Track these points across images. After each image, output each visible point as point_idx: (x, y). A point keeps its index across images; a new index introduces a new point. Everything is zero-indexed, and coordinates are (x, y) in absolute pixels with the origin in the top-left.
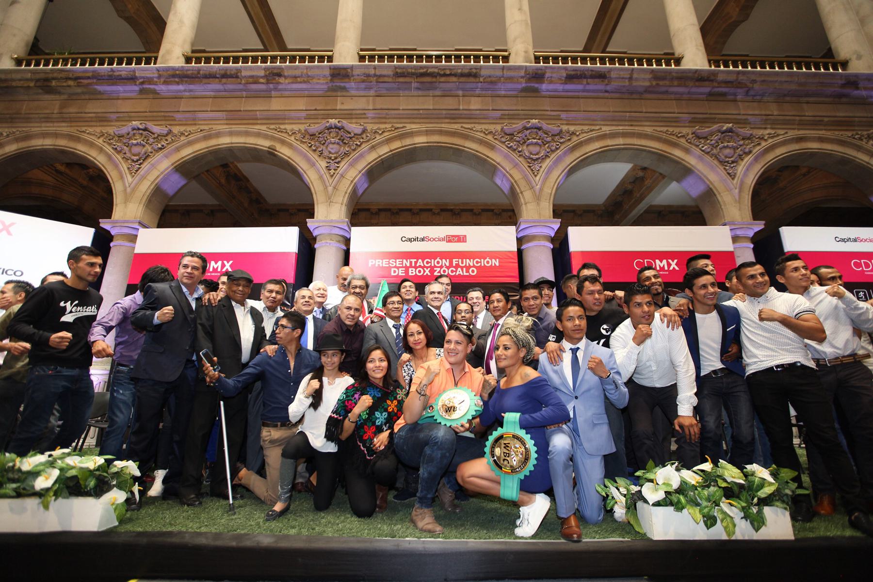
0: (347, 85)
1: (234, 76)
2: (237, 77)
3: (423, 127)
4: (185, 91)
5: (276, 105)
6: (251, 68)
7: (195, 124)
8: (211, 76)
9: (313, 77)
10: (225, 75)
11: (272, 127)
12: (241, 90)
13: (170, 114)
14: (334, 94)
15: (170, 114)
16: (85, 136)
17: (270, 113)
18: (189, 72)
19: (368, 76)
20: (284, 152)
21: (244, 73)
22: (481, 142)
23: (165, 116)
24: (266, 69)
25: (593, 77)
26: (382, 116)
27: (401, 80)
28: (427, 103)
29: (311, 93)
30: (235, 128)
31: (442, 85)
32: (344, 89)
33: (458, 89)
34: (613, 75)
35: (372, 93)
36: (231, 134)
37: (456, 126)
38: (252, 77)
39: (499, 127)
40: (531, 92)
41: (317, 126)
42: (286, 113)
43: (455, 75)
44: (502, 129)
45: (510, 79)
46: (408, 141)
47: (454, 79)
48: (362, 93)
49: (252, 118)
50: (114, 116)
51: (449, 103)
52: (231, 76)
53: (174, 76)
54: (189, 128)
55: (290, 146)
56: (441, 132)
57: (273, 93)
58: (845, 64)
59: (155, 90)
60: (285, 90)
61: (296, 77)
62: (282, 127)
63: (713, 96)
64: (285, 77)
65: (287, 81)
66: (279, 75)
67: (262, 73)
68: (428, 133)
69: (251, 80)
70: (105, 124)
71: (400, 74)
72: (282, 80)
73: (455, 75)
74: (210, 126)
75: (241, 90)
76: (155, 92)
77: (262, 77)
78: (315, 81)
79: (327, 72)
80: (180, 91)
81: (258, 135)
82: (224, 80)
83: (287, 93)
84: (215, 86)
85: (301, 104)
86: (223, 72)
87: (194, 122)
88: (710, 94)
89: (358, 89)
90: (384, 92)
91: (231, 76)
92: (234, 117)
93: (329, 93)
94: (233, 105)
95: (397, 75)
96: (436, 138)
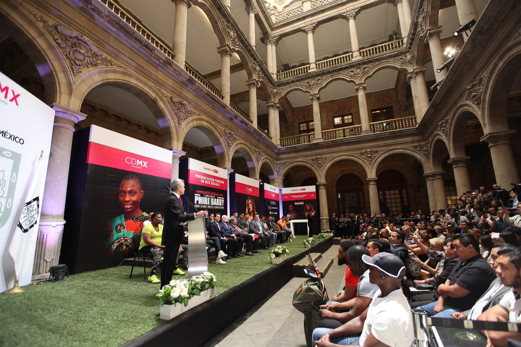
0: (189, 85)
1: (151, 50)
2: (151, 51)
3: (207, 119)
4: (114, 32)
5: (161, 76)
6: (161, 53)
7: (117, 59)
8: (139, 40)
9: (181, 75)
10: (147, 46)
11: (157, 87)
12: (146, 56)
13: (102, 41)
14: (182, 85)
15: (102, 41)
16: (21, 8)
17: (156, 78)
18: (128, 29)
19: (199, 88)
20: (161, 104)
21: (156, 52)
22: (219, 133)
23: (98, 41)
24: (166, 58)
25: (211, 97)
26: (197, 107)
27: (207, 96)
28: (208, 109)
29: (174, 79)
30: (141, 77)
31: (215, 105)
32: (187, 86)
33: (217, 108)
34: (249, 126)
35: (194, 93)
36: (137, 79)
37: (214, 123)
38: (158, 56)
39: (223, 129)
40: (231, 119)
41: (176, 99)
42: (165, 84)
43: (220, 104)
44: (224, 130)
45: (231, 113)
46: (214, 130)
47: (219, 105)
48: (191, 91)
49: (148, 76)
50: (56, 11)
51: (214, 112)
52: (149, 49)
53: (117, 24)
54: (114, 60)
55: (164, 103)
56: (211, 124)
57: (159, 68)
58: (271, 138)
59: (94, 16)
60: (165, 70)
61: (175, 70)
62: (162, 90)
63: (259, 140)
64: (172, 67)
65: (171, 69)
66: (170, 65)
67: (164, 59)
68: (207, 122)
69: (157, 57)
70: (44, 11)
71: (208, 94)
72: (169, 67)
73: (220, 104)
74: (127, 67)
75: (146, 56)
76: (93, 17)
77: (162, 60)
78: (181, 77)
79: (188, 77)
80: (111, 30)
81: (151, 88)
82: (144, 47)
83: (165, 72)
84: (137, 46)
85: (170, 82)
86: (146, 44)
87: (116, 57)
88: (258, 139)
89: (191, 89)
90: (198, 96)
91: (149, 49)
92: (140, 69)
93: (180, 83)
94: (141, 62)
95: (207, 94)
96: (209, 125)
